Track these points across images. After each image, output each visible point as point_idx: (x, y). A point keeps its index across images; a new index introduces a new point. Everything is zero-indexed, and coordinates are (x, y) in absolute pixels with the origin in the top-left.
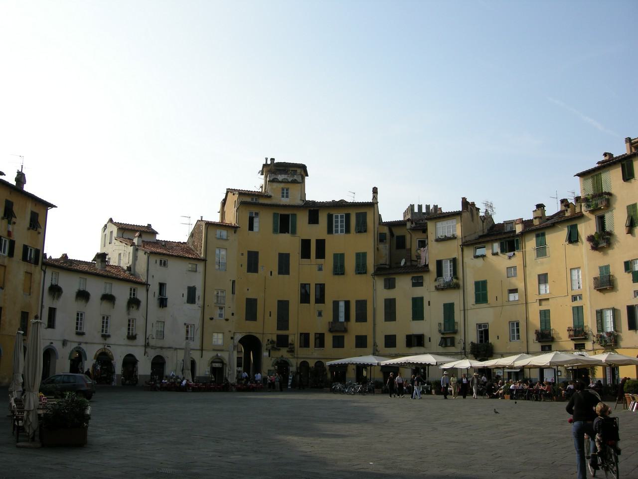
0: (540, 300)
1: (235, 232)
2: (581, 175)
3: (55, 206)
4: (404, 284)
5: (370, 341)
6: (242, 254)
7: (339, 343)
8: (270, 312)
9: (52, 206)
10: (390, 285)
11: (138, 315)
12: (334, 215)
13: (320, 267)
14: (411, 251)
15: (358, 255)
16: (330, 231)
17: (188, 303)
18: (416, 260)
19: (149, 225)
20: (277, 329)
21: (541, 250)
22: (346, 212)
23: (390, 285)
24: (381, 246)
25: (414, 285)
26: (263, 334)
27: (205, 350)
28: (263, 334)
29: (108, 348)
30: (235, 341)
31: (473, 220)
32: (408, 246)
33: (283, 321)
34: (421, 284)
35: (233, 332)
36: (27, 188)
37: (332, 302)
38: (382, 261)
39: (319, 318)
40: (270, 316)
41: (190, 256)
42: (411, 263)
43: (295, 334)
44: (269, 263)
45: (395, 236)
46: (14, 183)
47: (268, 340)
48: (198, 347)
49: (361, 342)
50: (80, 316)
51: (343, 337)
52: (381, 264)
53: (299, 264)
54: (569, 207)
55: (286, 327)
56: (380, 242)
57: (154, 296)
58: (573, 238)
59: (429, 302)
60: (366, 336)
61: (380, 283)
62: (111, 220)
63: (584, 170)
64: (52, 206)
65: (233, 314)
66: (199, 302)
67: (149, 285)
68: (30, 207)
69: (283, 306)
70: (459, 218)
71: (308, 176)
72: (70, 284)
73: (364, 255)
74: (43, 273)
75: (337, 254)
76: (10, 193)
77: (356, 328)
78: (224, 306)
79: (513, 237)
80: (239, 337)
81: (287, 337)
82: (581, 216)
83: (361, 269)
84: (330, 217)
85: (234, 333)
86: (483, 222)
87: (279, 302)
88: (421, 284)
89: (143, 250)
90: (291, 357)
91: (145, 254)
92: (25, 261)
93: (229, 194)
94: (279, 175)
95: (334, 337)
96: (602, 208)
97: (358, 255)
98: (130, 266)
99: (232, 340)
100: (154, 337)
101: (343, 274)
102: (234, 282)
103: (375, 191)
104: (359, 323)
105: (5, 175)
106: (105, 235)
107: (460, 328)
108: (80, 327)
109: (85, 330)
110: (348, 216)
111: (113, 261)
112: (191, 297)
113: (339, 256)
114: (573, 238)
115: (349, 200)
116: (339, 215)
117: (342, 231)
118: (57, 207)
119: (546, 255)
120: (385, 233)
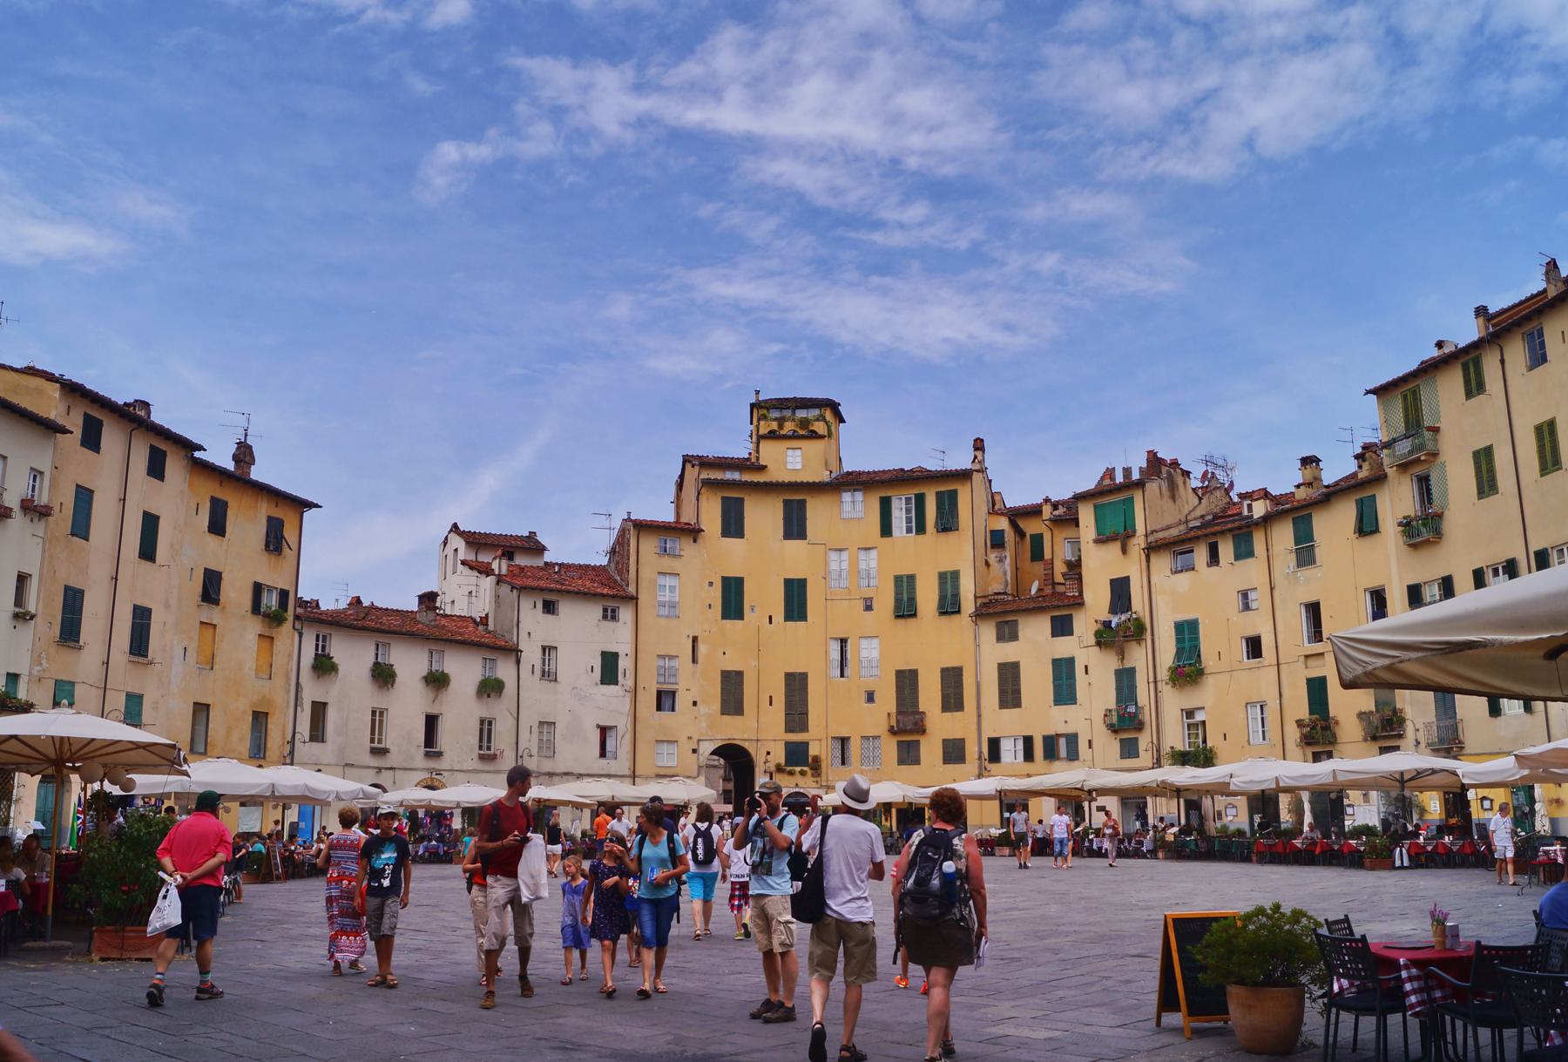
0: (1307, 657)
1: (695, 541)
2: (1381, 391)
3: (317, 506)
4: (1035, 629)
5: (971, 751)
6: (711, 584)
7: (909, 755)
8: (771, 697)
9: (311, 505)
10: (1007, 633)
11: (500, 711)
12: (893, 498)
14: (1052, 564)
15: (942, 577)
16: (886, 530)
17: (602, 684)
18: (1064, 582)
19: (532, 534)
20: (786, 732)
21: (1305, 555)
22: (917, 491)
23: (1007, 633)
24: (993, 557)
27: (640, 777)
29: (436, 777)
30: (701, 759)
31: (1173, 497)
32: (1047, 555)
33: (797, 716)
34: (1072, 634)
35: (695, 738)
36: (257, 474)
38: (998, 588)
39: (869, 705)
40: (771, 704)
41: (605, 591)
42: (1053, 588)
43: (820, 740)
44: (765, 597)
45: (1028, 537)
46: (230, 465)
47: (768, 753)
48: (627, 772)
49: (954, 752)
50: (378, 716)
51: (918, 742)
52: (996, 594)
54: (1364, 461)
55: (804, 727)
56: (993, 546)
57: (533, 673)
58: (1367, 526)
59: (1086, 667)
60: (964, 739)
61: (988, 631)
62: (455, 526)
63: (1383, 381)
64: (311, 505)
65: (695, 704)
66: (626, 681)
67: (521, 651)
68: (264, 510)
69: (796, 685)
70: (1141, 492)
71: (845, 422)
72: (354, 657)
73: (955, 575)
74: (297, 635)
75: (901, 577)
76: (221, 485)
77: (941, 725)
79: (1248, 527)
80: (707, 748)
81: (807, 744)
82: (1379, 479)
83: (949, 606)
85: (699, 741)
86: (1200, 499)
87: (790, 677)
89: (509, 583)
90: (814, 785)
91: (512, 591)
92: (256, 614)
93: (688, 466)
95: (898, 742)
96: (1423, 458)
97: (942, 577)
98: (487, 615)
99: (696, 755)
100: (534, 751)
101: (914, 615)
102: (695, 639)
103: (979, 445)
104: (948, 715)
105: (205, 450)
106: (446, 556)
107: (1148, 716)
108: (379, 739)
109: (388, 742)
110: (920, 500)
111: (445, 605)
112: (609, 668)
113: (905, 579)
114: (1367, 526)
115: (933, 465)
117: (909, 530)
118: (321, 507)
119: (1314, 563)
120: (1003, 530)
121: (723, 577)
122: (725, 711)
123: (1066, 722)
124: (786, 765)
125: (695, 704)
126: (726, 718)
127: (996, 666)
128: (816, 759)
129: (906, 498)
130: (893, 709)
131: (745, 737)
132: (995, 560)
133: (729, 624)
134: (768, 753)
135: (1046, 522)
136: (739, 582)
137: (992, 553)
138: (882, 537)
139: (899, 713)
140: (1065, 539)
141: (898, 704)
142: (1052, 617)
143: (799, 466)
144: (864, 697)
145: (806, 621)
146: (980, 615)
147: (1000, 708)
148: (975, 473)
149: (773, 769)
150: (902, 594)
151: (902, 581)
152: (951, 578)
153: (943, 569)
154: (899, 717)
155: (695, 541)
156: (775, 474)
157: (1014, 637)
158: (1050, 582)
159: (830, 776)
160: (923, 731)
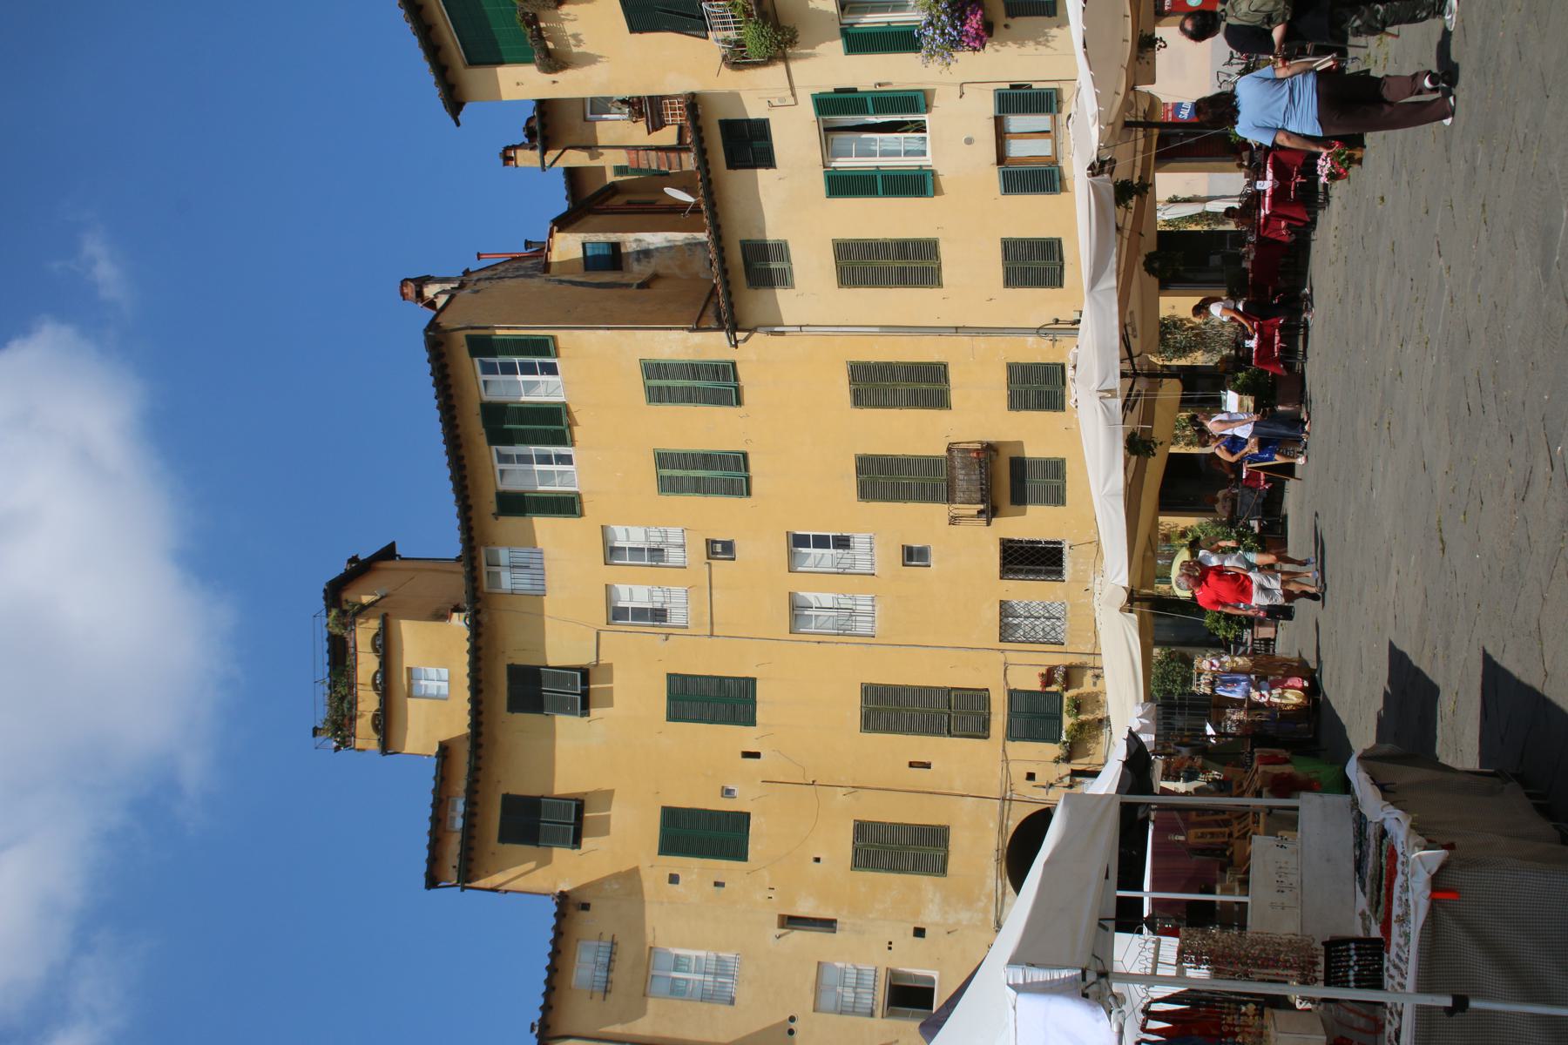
1: (586, 907)
5: (1035, 351)
6: (674, 879)
8: (911, 765)
13: (719, 548)
14: (636, 148)
16: (566, 505)
25: (767, 160)
26: (1004, 799)
28: (1004, 799)
37: (863, 504)
40: (927, 766)
47: (1031, 776)
53: (712, 635)
55: (979, 698)
65: (919, 932)
71: (393, 544)
73: (653, 370)
78: (882, 974)
81: (1013, 694)
84: (517, 504)
88: (760, 130)
94: (361, 707)
97: (656, 396)
102: (791, 922)
104: (955, 396)
113: (667, 472)
116: (499, 467)
117: (566, 459)
121: (659, 854)
122: (940, 868)
123: (969, 141)
124: (1055, 739)
125: (919, 932)
126: (951, 868)
127: (845, 291)
128: (1048, 678)
129: (500, 462)
130: (940, 511)
131: (993, 825)
132: (644, 262)
133: (756, 844)
134: (1031, 776)
135: (547, 163)
136: (671, 817)
137: (630, 271)
138: (581, 515)
139: (950, 500)
140: (585, 120)
141: (934, 498)
142: (733, 164)
143: (444, 673)
144: (915, 572)
145: (754, 680)
146: (732, 323)
147: (940, 285)
148: (438, 320)
149: (1065, 769)
150: (698, 479)
151: (670, 478)
152: (660, 378)
153: (642, 395)
154: (959, 495)
155: (586, 907)
156: (457, 723)
157: (781, 250)
158: (673, 156)
159: (1082, 649)
160: (990, 450)
